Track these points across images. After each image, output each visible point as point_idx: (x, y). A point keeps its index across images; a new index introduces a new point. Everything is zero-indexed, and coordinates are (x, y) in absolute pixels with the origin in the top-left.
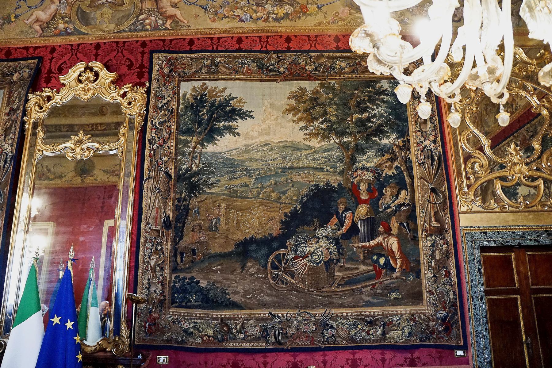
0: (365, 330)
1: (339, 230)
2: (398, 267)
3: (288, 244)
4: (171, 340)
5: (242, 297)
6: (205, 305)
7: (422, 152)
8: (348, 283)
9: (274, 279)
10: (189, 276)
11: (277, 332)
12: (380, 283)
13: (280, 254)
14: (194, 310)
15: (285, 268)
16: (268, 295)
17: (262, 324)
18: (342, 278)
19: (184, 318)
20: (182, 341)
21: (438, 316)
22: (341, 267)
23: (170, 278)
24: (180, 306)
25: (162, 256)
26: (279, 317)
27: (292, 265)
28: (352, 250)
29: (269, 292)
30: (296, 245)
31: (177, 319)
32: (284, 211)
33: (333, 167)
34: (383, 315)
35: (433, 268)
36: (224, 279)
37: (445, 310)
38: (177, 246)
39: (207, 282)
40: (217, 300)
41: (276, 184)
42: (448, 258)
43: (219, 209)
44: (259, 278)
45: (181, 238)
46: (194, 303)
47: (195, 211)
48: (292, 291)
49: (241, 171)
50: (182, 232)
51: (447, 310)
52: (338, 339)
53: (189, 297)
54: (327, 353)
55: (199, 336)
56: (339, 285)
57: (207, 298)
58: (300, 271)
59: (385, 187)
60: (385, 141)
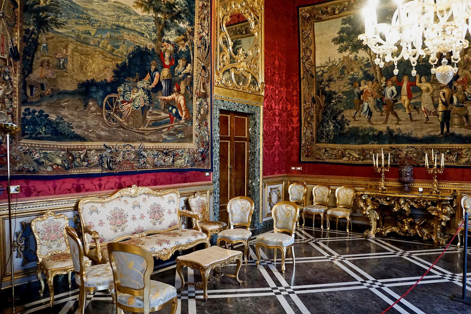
0: (162, 159)
1: (150, 85)
2: (183, 116)
3: (118, 90)
4: (22, 170)
5: (85, 131)
6: (55, 137)
7: (200, 39)
8: (154, 125)
9: (107, 117)
10: (38, 109)
11: (109, 160)
12: (172, 126)
13: (112, 97)
14: (44, 141)
15: (115, 109)
16: (103, 130)
17: (99, 154)
18: (151, 121)
19: (35, 149)
20: (34, 170)
21: (199, 150)
22: (150, 112)
23: (20, 110)
24: (30, 138)
25: (10, 87)
26: (110, 148)
27: (121, 107)
28: (157, 101)
29: (104, 127)
30: (124, 92)
31: (28, 150)
32: (117, 62)
33: (150, 35)
34: (173, 148)
35: (199, 119)
36: (69, 115)
37: (203, 147)
38: (27, 79)
39: (57, 116)
40: (64, 133)
41: (110, 38)
42: (207, 114)
43: (67, 50)
44: (97, 115)
45: (30, 71)
46: (43, 135)
47: (44, 47)
48: (120, 128)
49: (85, 19)
50: (31, 65)
51: (204, 147)
52: (148, 165)
53: (39, 129)
54: (140, 175)
55: (50, 165)
56: (149, 126)
57: (56, 131)
58: (125, 113)
59: (180, 59)
60: (181, 25)
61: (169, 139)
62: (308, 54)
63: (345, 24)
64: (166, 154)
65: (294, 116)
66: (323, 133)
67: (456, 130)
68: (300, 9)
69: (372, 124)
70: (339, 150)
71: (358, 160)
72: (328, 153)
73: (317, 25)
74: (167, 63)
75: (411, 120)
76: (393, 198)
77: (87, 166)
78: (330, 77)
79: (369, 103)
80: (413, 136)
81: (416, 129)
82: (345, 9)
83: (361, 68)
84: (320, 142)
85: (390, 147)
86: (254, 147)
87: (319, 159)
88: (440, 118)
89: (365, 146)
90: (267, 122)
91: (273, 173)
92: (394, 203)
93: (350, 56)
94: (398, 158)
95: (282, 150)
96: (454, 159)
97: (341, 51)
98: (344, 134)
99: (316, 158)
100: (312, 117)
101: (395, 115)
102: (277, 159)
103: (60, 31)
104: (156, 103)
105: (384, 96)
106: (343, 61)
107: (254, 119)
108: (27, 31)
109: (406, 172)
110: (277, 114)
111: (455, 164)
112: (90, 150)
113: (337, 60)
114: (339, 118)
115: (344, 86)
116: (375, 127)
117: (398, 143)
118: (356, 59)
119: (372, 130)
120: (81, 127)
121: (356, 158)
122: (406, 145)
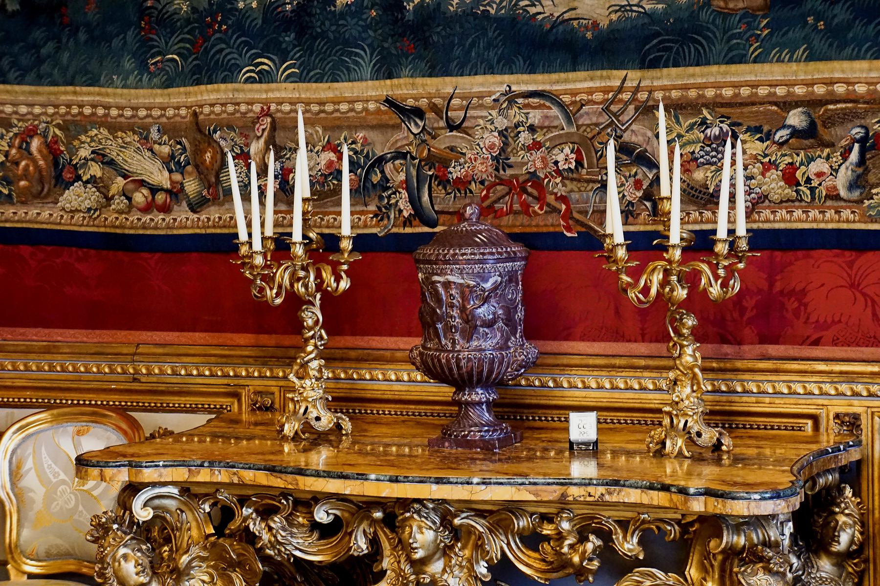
70: (31, 133)
71: (165, 209)
85: (390, 102)
92: (374, 542)
94: (444, 181)
96: (844, 175)
109: (466, 292)
117: (435, 70)
121: (154, 190)
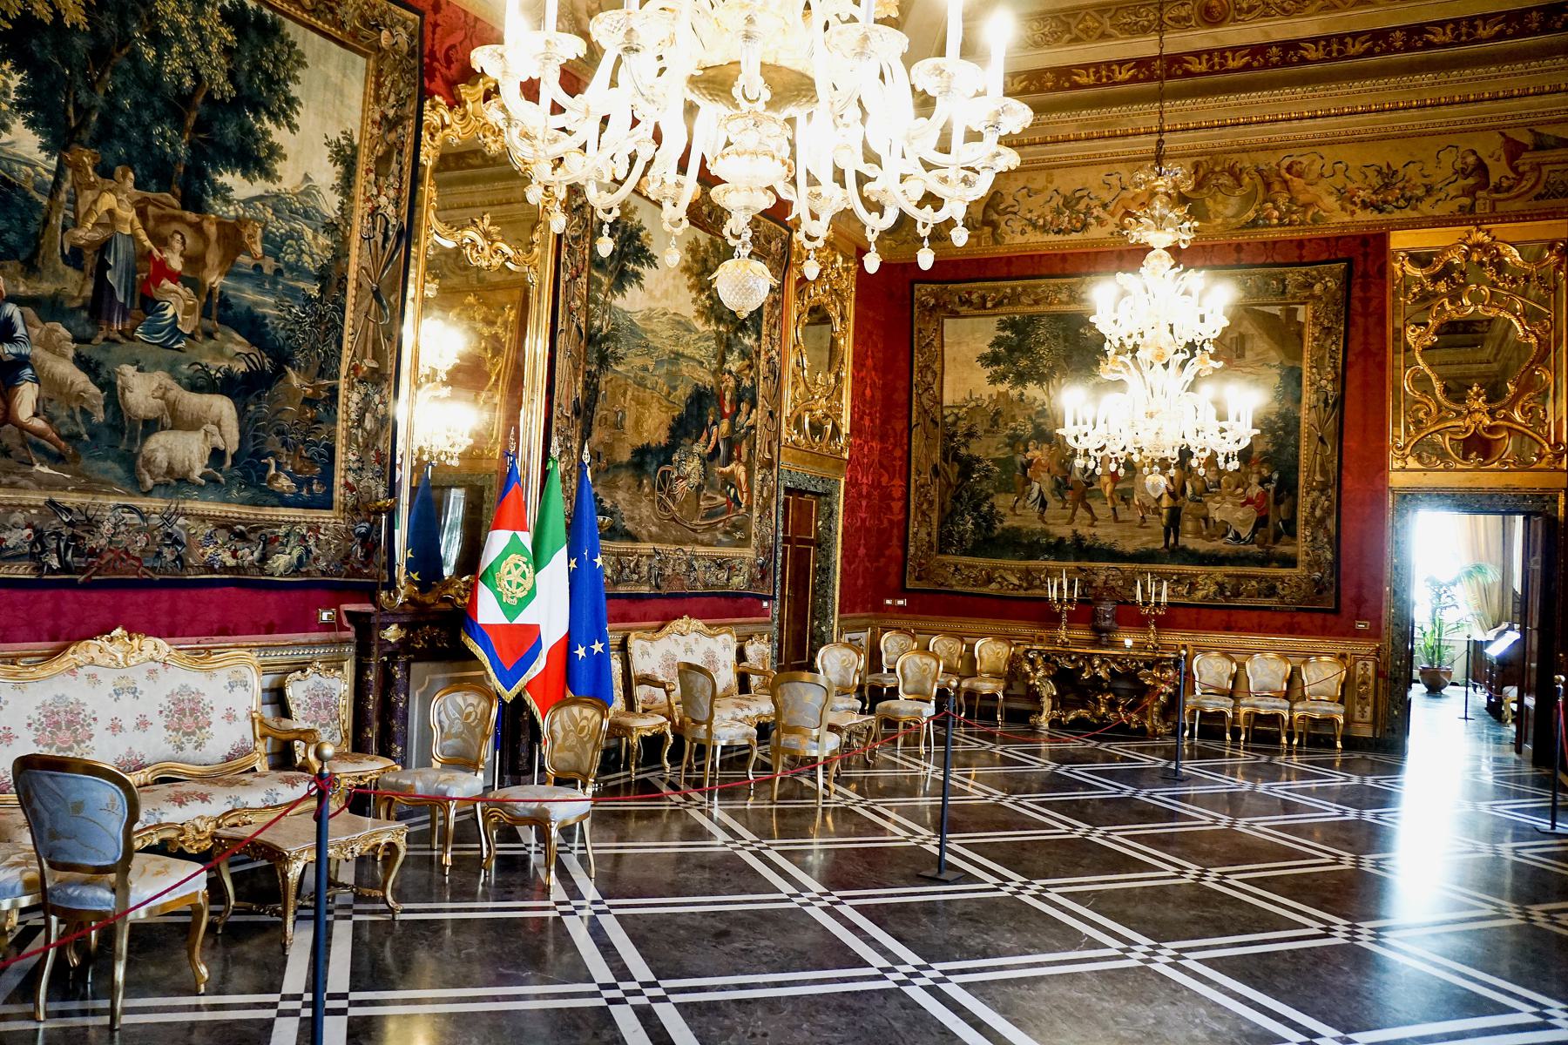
8: (708, 517)
50: (591, 425)
58: (679, 497)
60: (747, 341)
61: (725, 540)
62: (929, 378)
63: (1003, 329)
64: (720, 566)
65: (894, 499)
66: (951, 536)
67: (1189, 541)
68: (917, 286)
69: (1045, 523)
72: (961, 574)
73: (948, 323)
74: (727, 410)
75: (1116, 519)
76: (1081, 656)
77: (637, 581)
78: (970, 429)
79: (1041, 484)
80: (1119, 548)
81: (1123, 537)
82: (1006, 301)
83: (1030, 418)
84: (946, 553)
86: (828, 557)
87: (942, 584)
88: (1164, 520)
89: (1032, 563)
90: (850, 510)
91: (853, 611)
93: (1011, 392)
95: (868, 564)
97: (994, 380)
98: (993, 539)
99: (936, 583)
100: (931, 503)
101: (1089, 509)
102: (860, 582)
103: (619, 369)
104: (711, 478)
105: (1070, 473)
106: (997, 401)
107: (829, 504)
108: (589, 372)
110: (864, 492)
111: (1186, 601)
112: (642, 556)
113: (985, 397)
114: (985, 508)
115: (997, 449)
116: (1051, 529)
118: (1022, 400)
119: (1046, 534)
120: (632, 519)
122: (1106, 565)
